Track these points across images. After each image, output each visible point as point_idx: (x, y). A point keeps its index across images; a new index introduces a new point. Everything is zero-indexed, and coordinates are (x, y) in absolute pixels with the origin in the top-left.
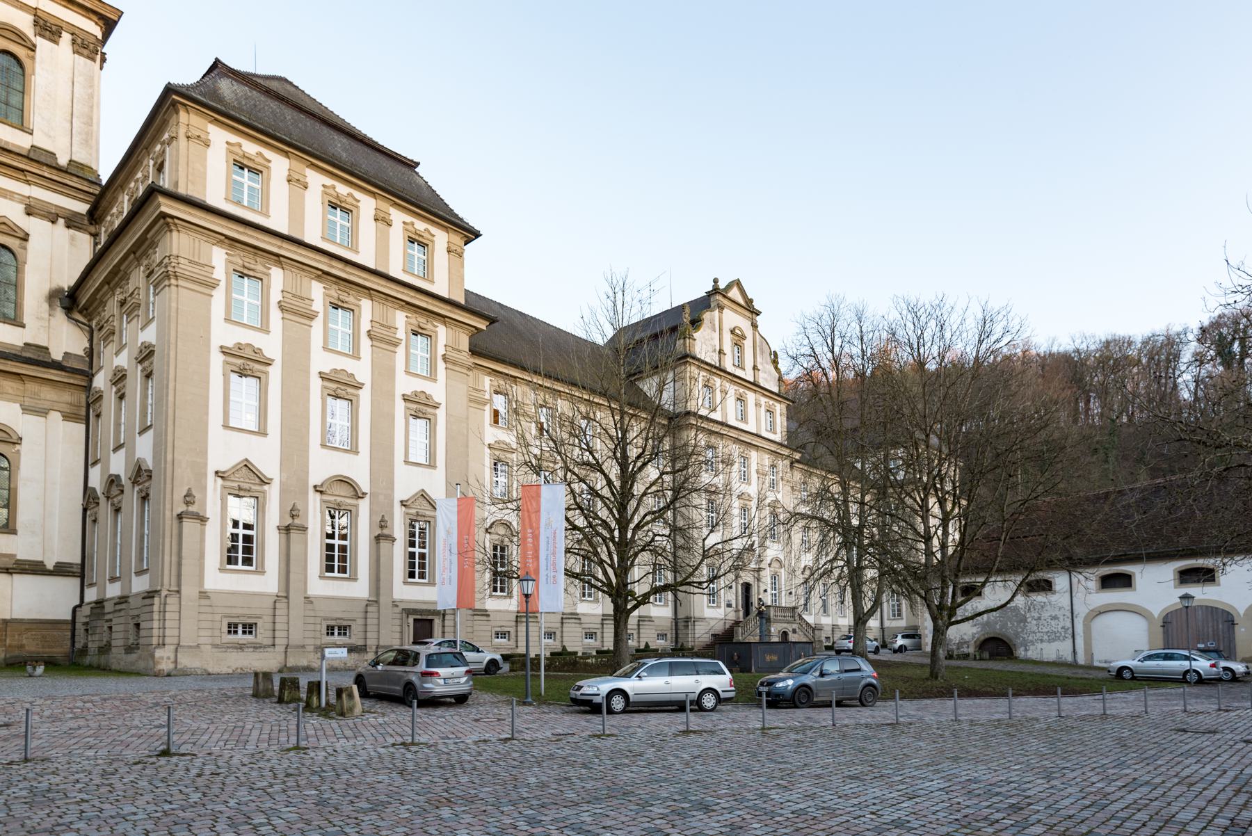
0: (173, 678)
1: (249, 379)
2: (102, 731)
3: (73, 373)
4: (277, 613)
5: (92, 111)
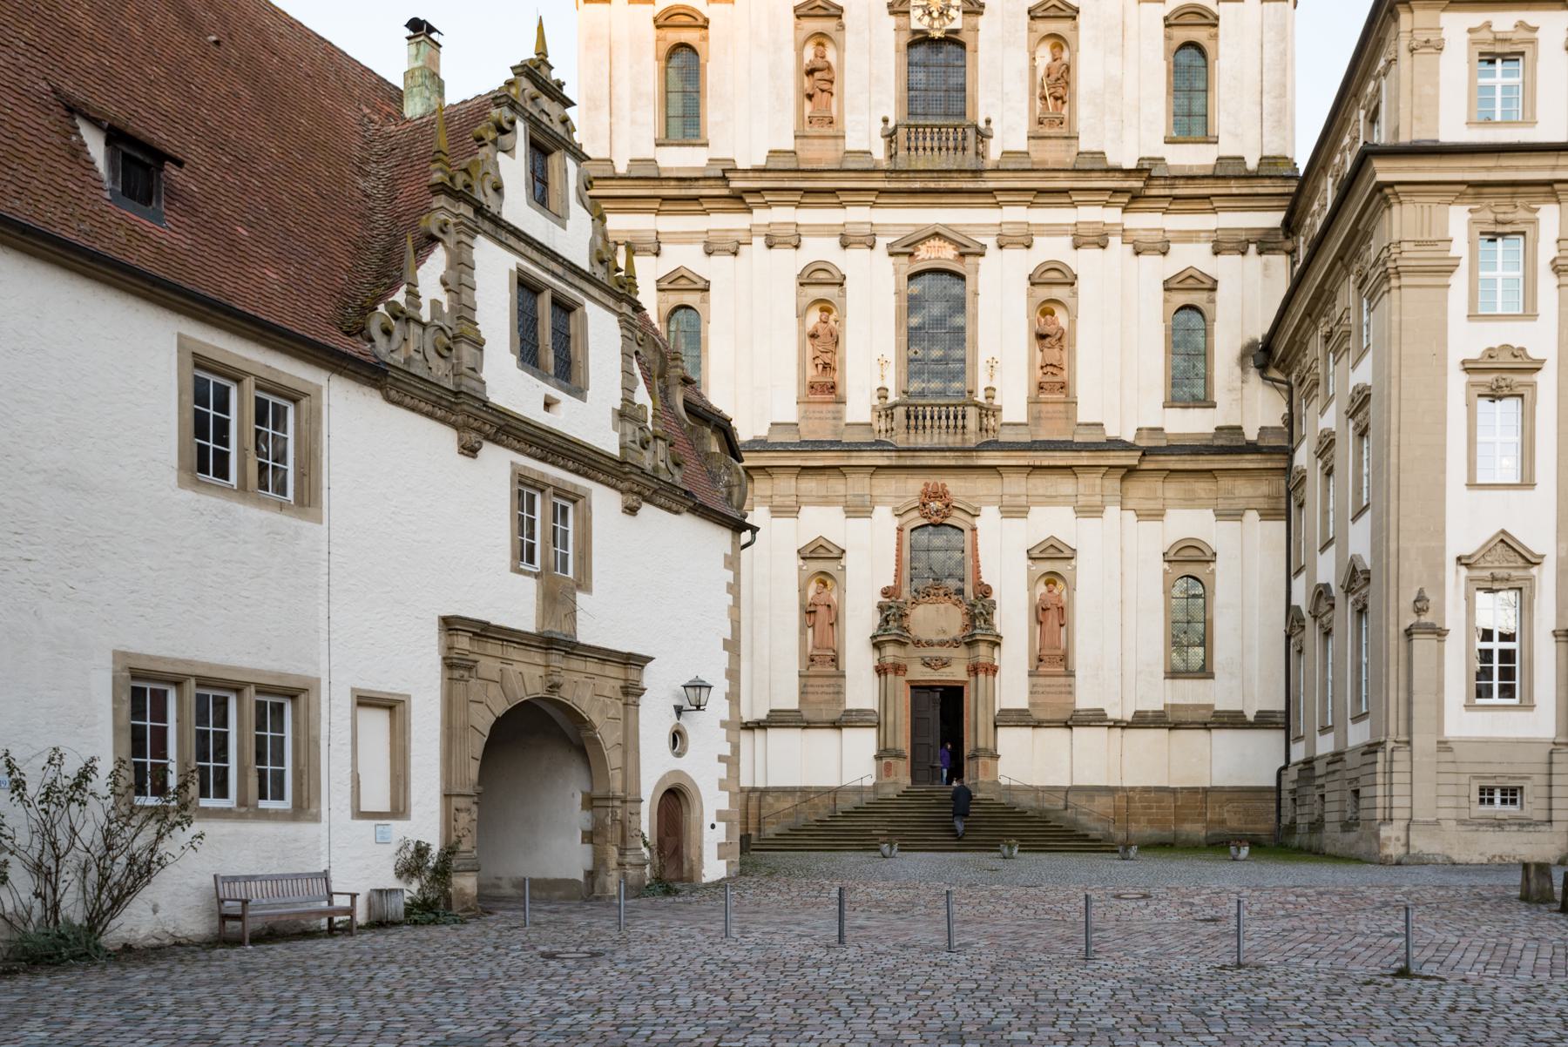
0: (1405, 868)
1: (1505, 401)
2: (1321, 936)
3: (1271, 453)
4: (1554, 771)
5: (1285, 75)
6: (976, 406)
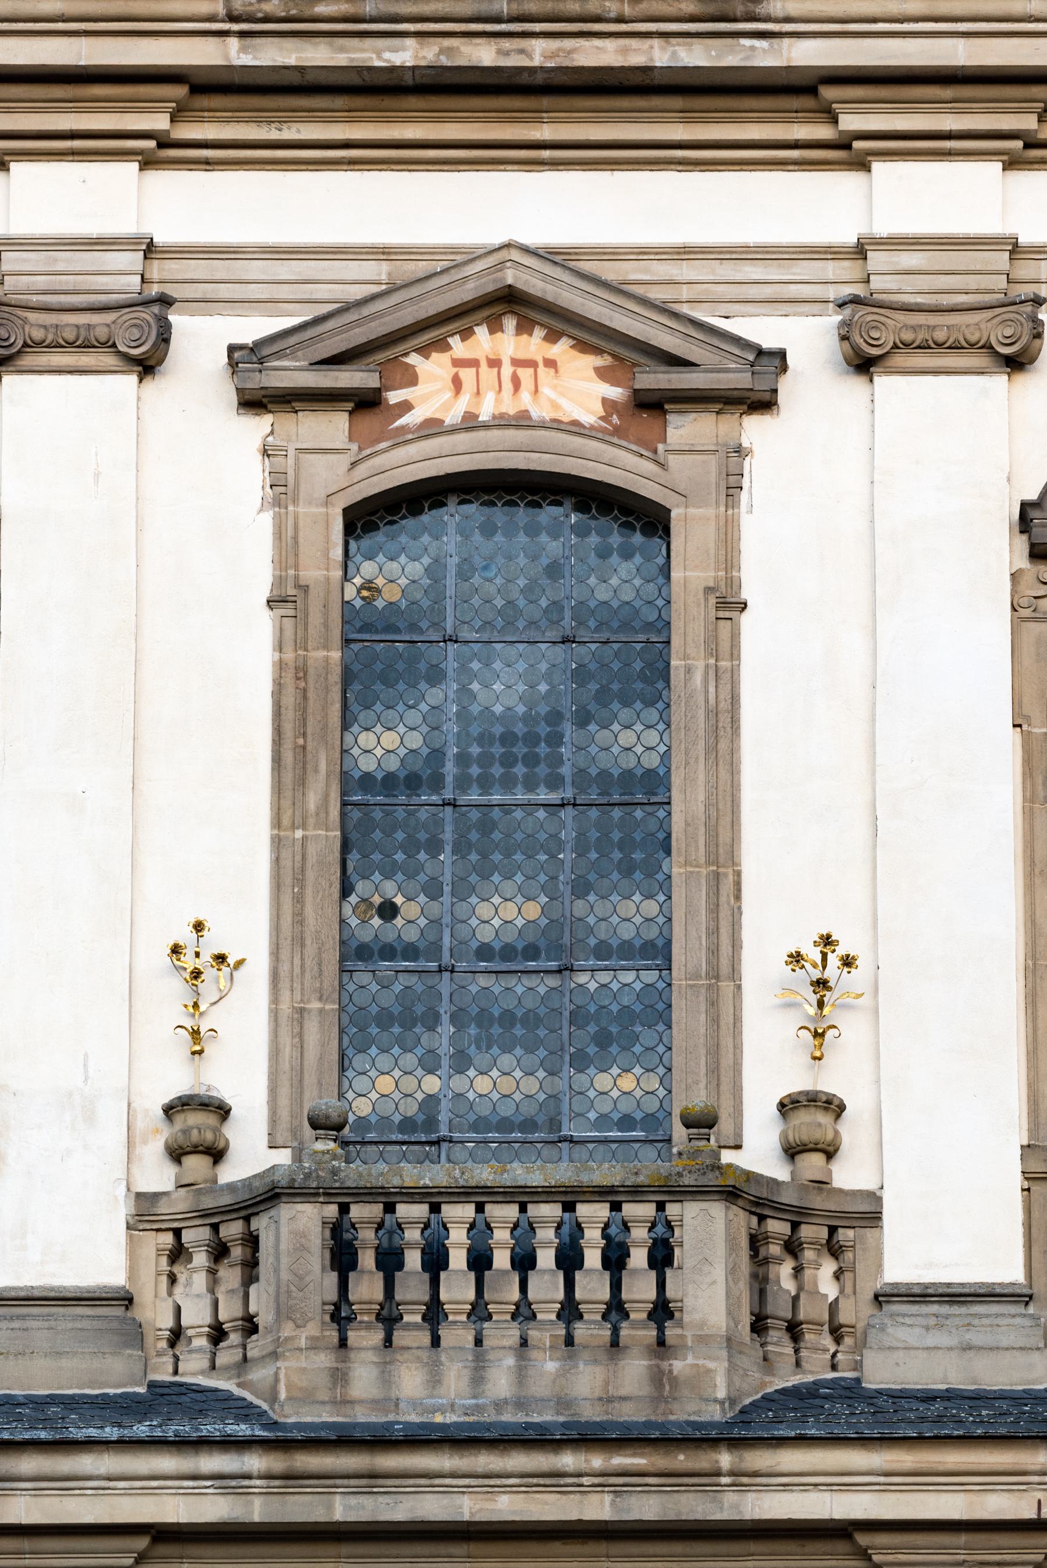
6: (731, 1194)
